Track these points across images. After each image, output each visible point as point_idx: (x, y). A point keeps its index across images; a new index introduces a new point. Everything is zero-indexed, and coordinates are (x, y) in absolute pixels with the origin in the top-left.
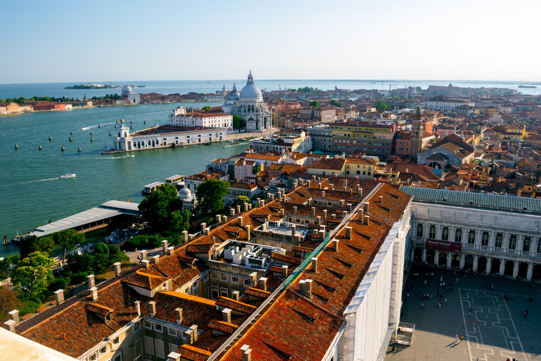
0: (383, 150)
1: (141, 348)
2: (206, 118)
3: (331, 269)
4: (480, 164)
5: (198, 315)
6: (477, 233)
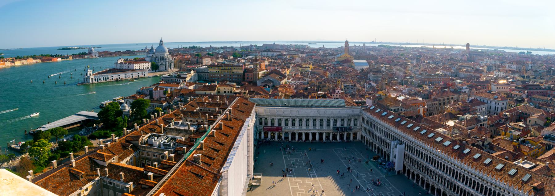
0: (238, 79)
4: (289, 84)
5: (133, 176)
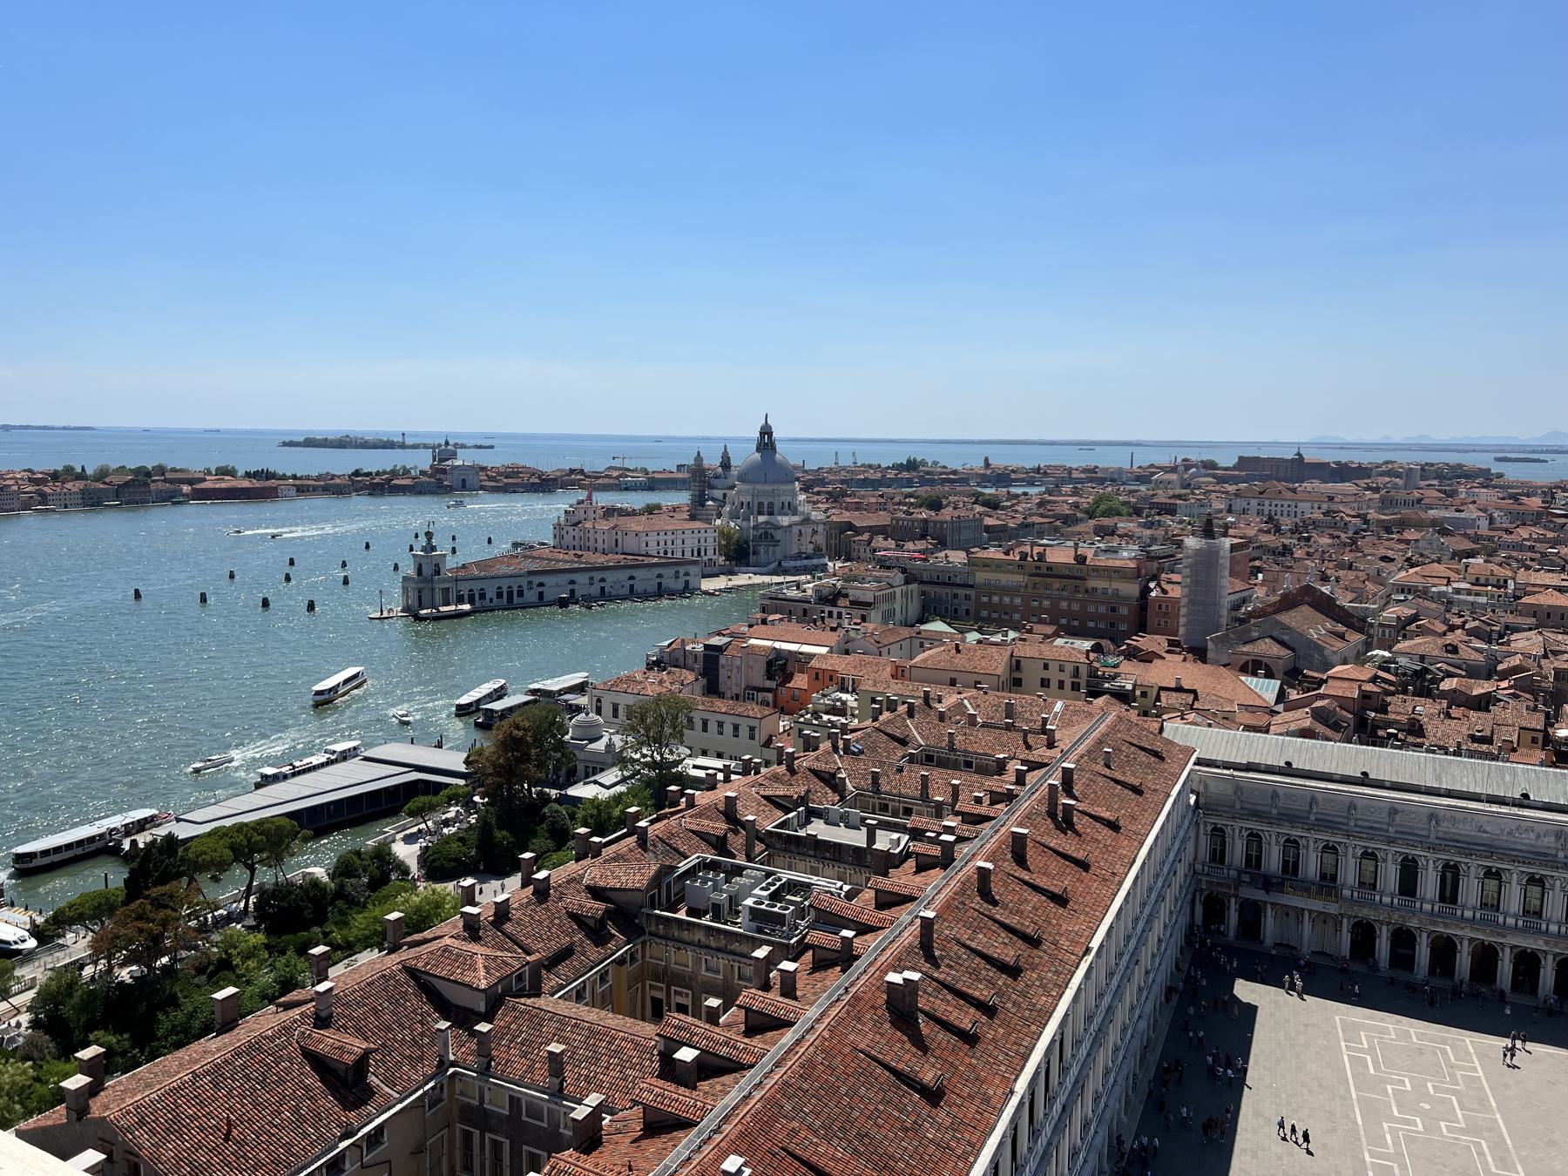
1: (445, 1160)
3: (973, 945)
6: (1385, 861)
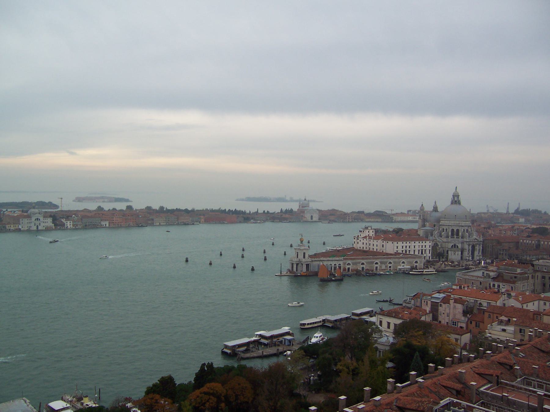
2: (399, 243)
